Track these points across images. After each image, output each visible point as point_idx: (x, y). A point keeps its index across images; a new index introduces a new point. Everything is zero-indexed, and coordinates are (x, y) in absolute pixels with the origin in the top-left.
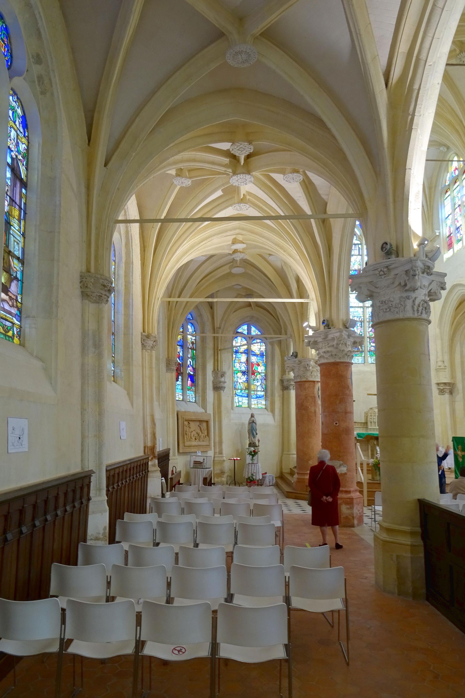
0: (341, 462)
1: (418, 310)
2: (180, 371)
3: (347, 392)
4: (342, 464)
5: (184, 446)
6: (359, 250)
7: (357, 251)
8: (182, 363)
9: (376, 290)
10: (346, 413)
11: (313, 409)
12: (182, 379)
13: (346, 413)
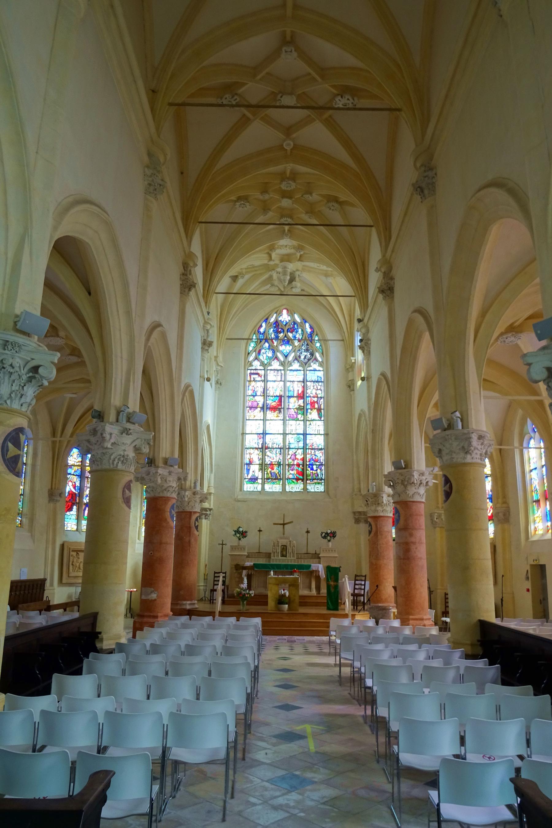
0: (152, 589)
1: (113, 463)
2: (76, 500)
3: (164, 524)
4: (153, 591)
5: (69, 577)
6: (281, 376)
7: (280, 376)
8: (79, 493)
9: (91, 447)
10: (161, 543)
11: (187, 539)
12: (78, 510)
13: (161, 543)
